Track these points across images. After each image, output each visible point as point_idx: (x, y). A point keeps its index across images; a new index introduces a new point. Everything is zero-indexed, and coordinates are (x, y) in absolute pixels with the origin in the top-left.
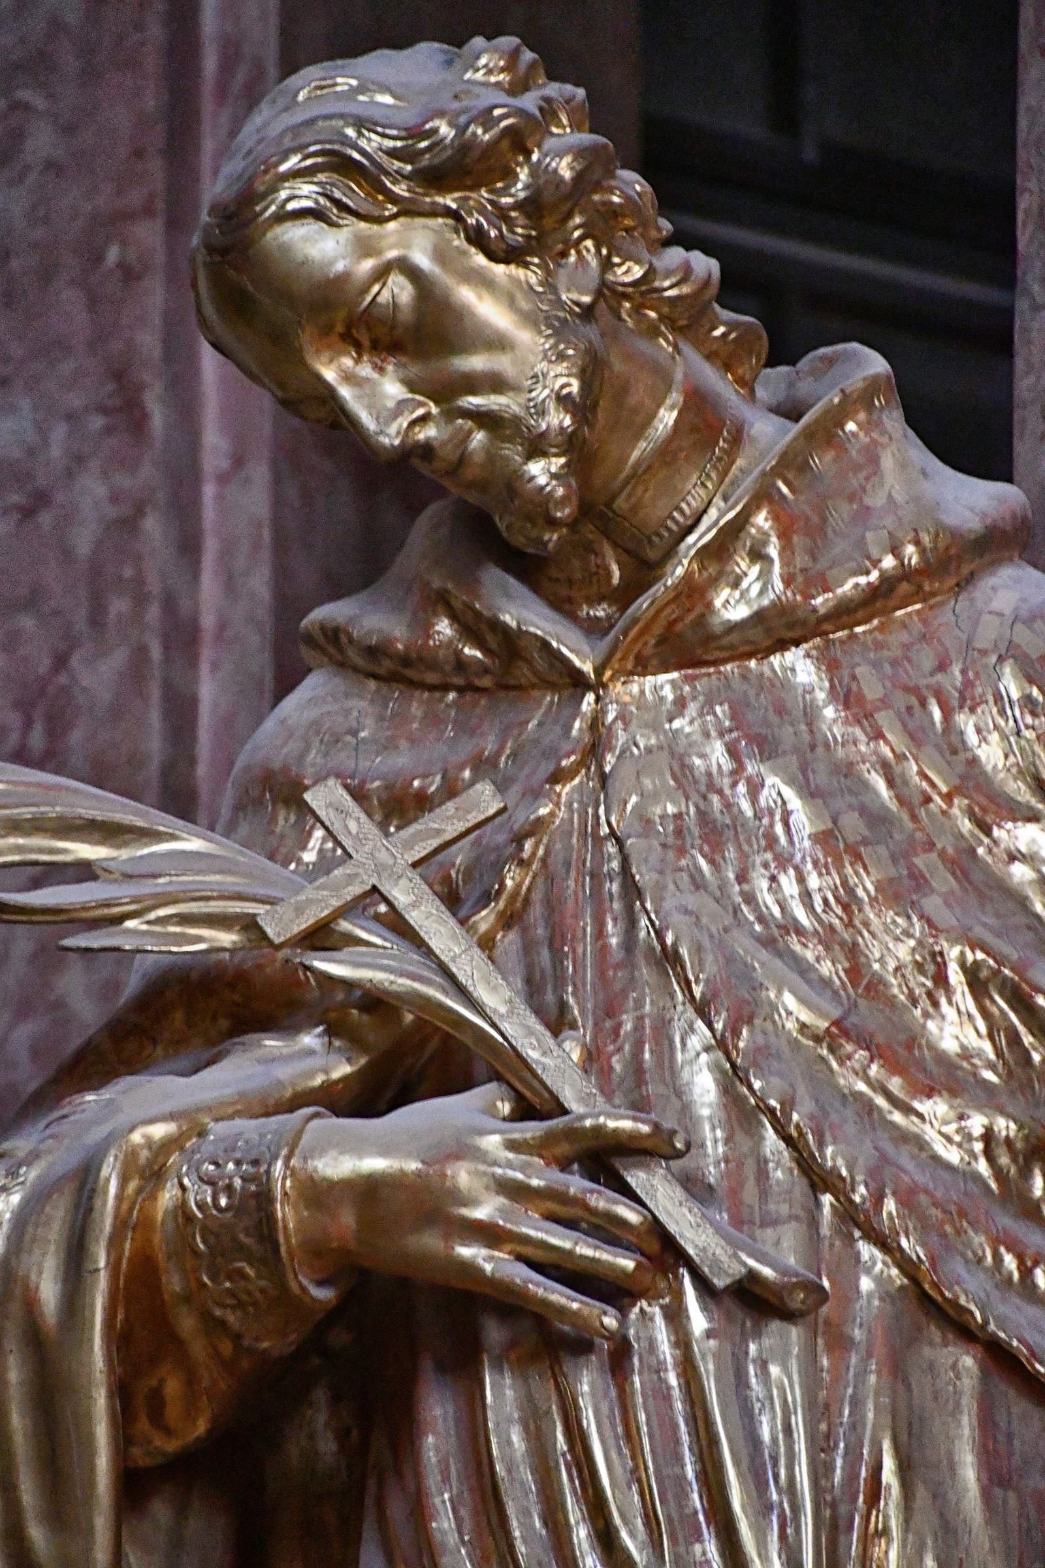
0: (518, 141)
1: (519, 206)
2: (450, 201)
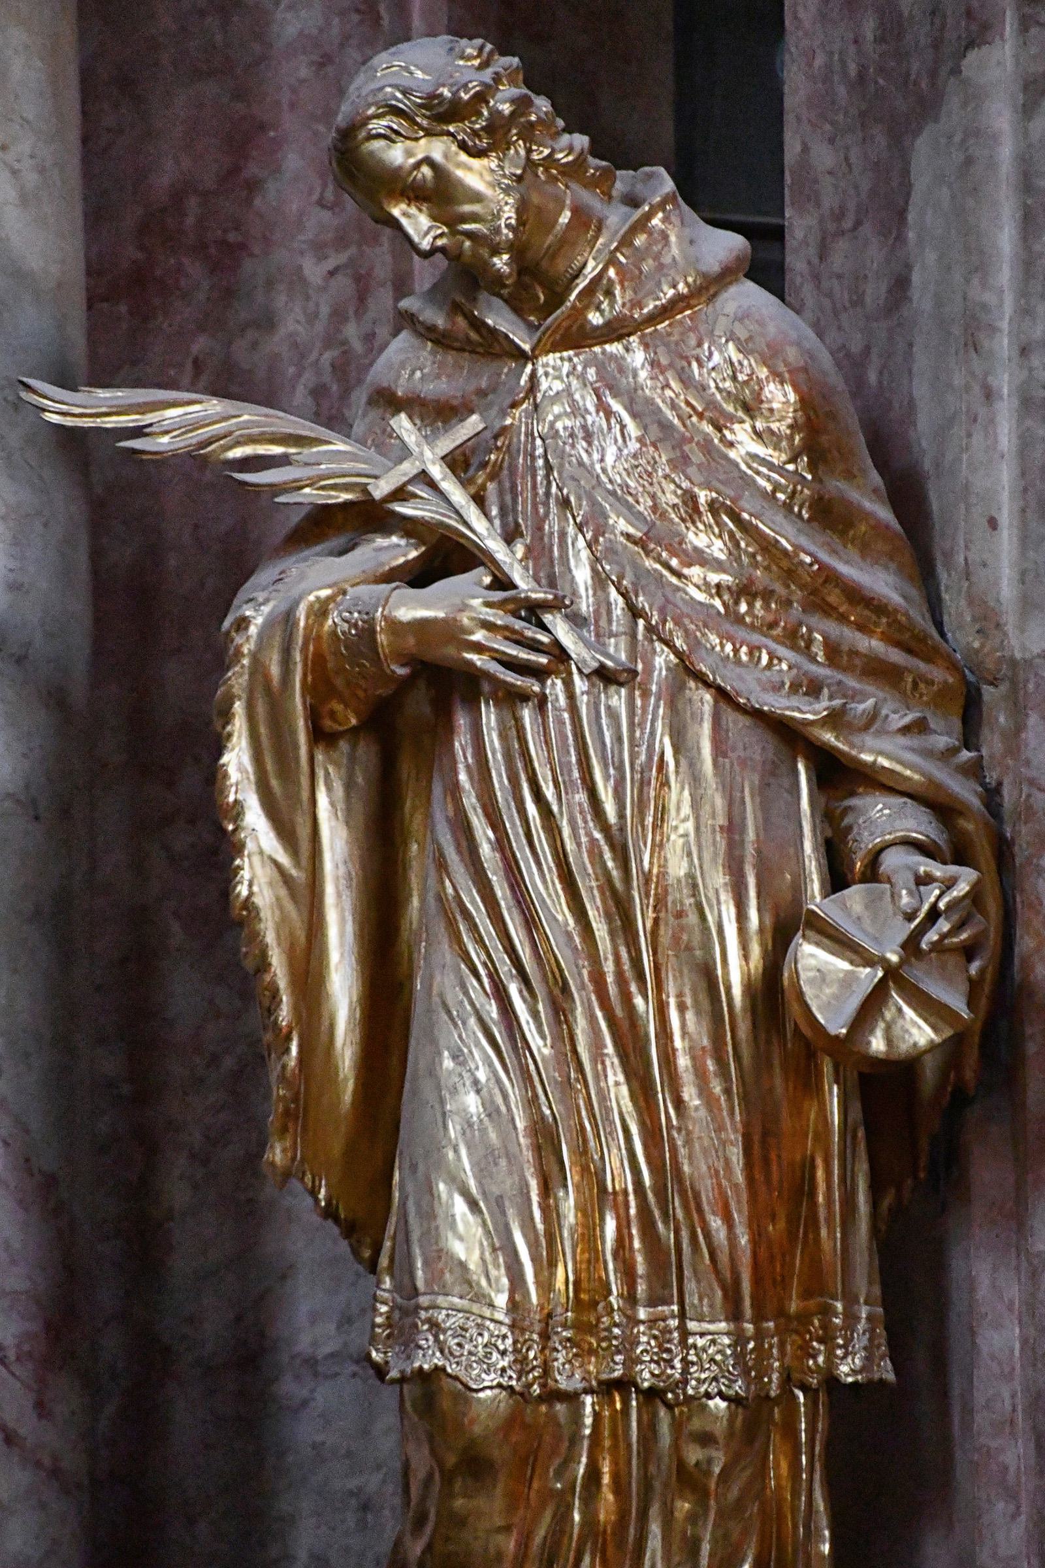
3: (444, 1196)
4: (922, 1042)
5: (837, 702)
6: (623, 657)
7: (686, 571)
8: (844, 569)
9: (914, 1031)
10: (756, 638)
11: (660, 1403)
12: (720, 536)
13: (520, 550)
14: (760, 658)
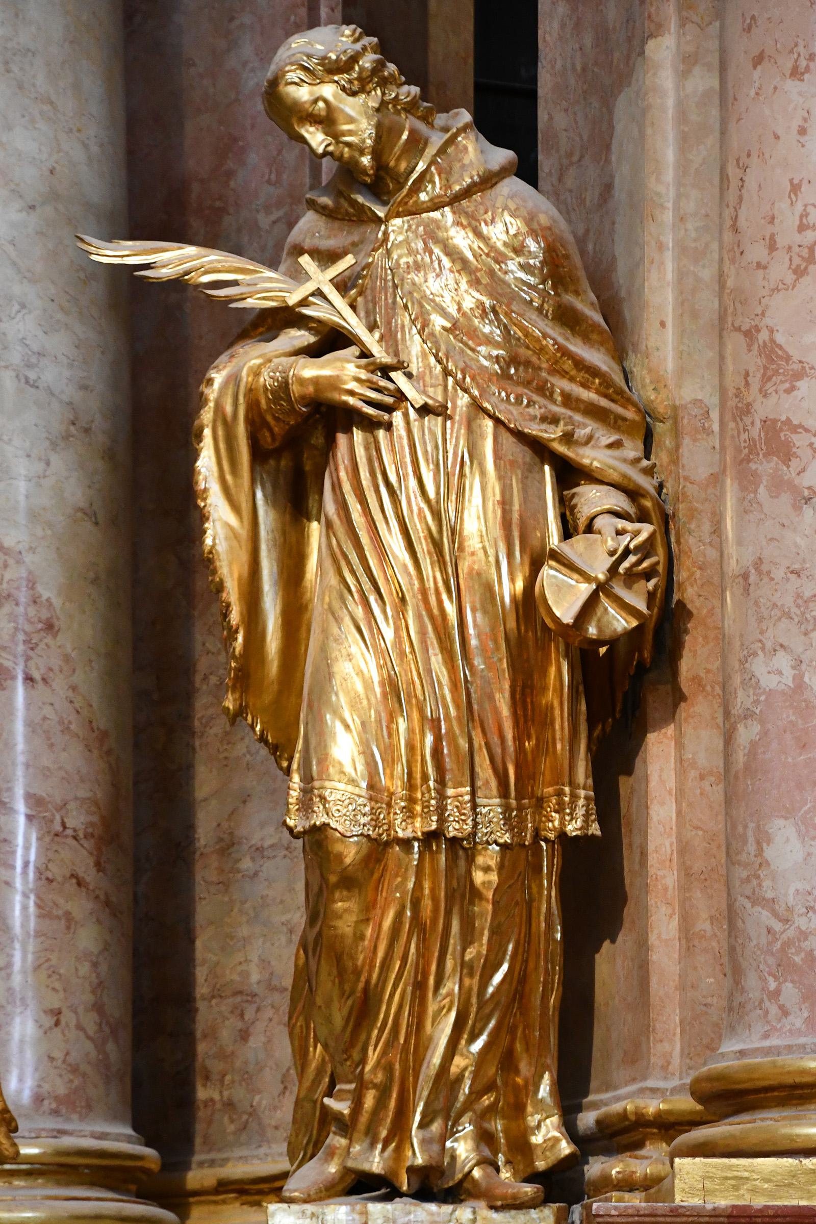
0: (354, 59)
1: (356, 79)
2: (336, 78)
3: (329, 722)
4: (619, 629)
5: (570, 428)
6: (440, 398)
7: (479, 348)
8: (572, 348)
9: (615, 622)
10: (520, 390)
11: (458, 847)
12: (498, 327)
13: (377, 335)
14: (522, 401)
